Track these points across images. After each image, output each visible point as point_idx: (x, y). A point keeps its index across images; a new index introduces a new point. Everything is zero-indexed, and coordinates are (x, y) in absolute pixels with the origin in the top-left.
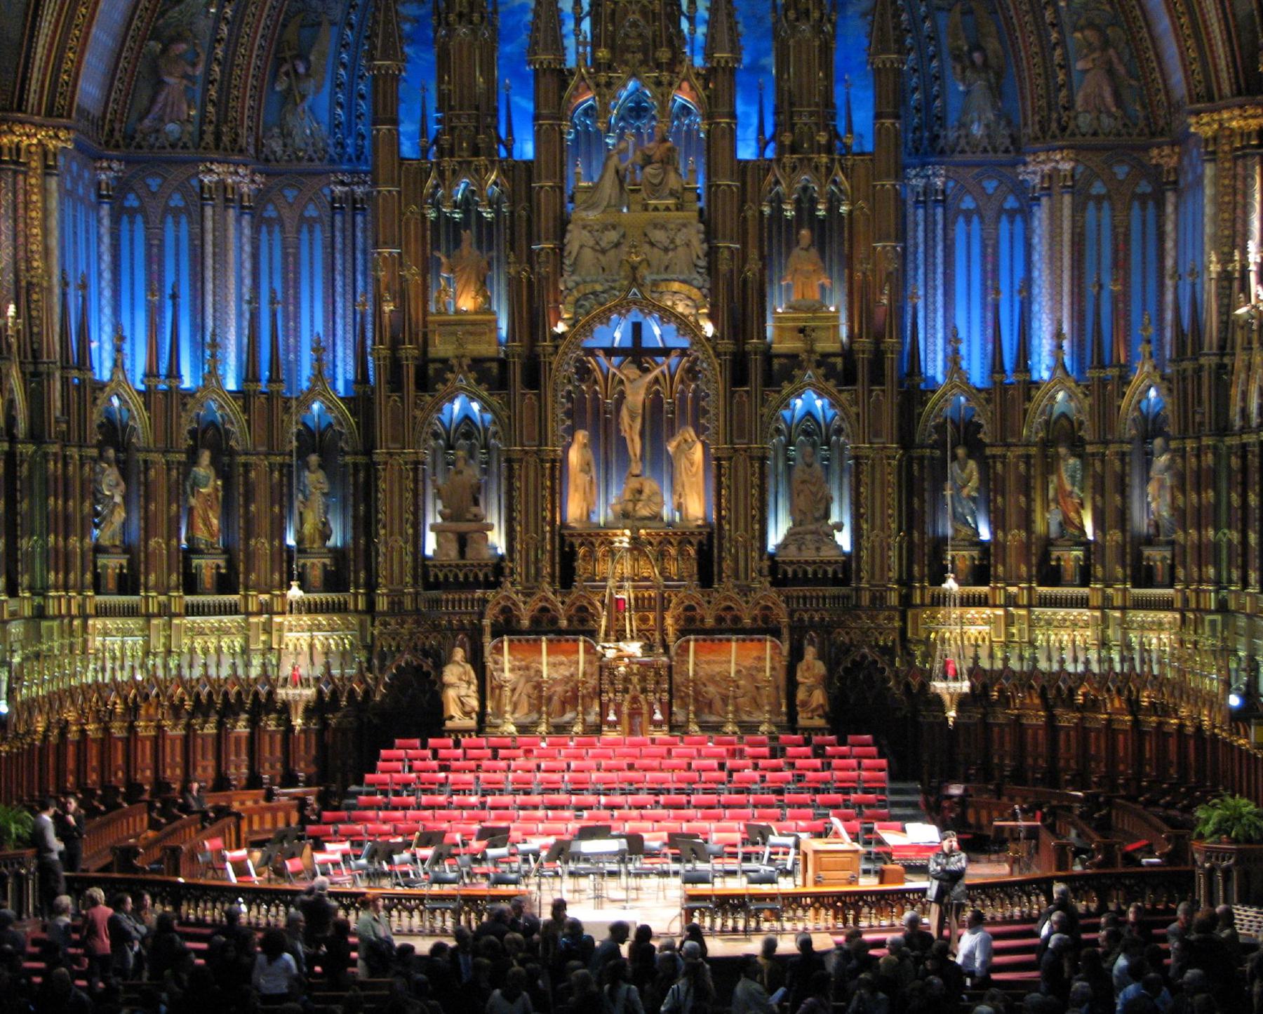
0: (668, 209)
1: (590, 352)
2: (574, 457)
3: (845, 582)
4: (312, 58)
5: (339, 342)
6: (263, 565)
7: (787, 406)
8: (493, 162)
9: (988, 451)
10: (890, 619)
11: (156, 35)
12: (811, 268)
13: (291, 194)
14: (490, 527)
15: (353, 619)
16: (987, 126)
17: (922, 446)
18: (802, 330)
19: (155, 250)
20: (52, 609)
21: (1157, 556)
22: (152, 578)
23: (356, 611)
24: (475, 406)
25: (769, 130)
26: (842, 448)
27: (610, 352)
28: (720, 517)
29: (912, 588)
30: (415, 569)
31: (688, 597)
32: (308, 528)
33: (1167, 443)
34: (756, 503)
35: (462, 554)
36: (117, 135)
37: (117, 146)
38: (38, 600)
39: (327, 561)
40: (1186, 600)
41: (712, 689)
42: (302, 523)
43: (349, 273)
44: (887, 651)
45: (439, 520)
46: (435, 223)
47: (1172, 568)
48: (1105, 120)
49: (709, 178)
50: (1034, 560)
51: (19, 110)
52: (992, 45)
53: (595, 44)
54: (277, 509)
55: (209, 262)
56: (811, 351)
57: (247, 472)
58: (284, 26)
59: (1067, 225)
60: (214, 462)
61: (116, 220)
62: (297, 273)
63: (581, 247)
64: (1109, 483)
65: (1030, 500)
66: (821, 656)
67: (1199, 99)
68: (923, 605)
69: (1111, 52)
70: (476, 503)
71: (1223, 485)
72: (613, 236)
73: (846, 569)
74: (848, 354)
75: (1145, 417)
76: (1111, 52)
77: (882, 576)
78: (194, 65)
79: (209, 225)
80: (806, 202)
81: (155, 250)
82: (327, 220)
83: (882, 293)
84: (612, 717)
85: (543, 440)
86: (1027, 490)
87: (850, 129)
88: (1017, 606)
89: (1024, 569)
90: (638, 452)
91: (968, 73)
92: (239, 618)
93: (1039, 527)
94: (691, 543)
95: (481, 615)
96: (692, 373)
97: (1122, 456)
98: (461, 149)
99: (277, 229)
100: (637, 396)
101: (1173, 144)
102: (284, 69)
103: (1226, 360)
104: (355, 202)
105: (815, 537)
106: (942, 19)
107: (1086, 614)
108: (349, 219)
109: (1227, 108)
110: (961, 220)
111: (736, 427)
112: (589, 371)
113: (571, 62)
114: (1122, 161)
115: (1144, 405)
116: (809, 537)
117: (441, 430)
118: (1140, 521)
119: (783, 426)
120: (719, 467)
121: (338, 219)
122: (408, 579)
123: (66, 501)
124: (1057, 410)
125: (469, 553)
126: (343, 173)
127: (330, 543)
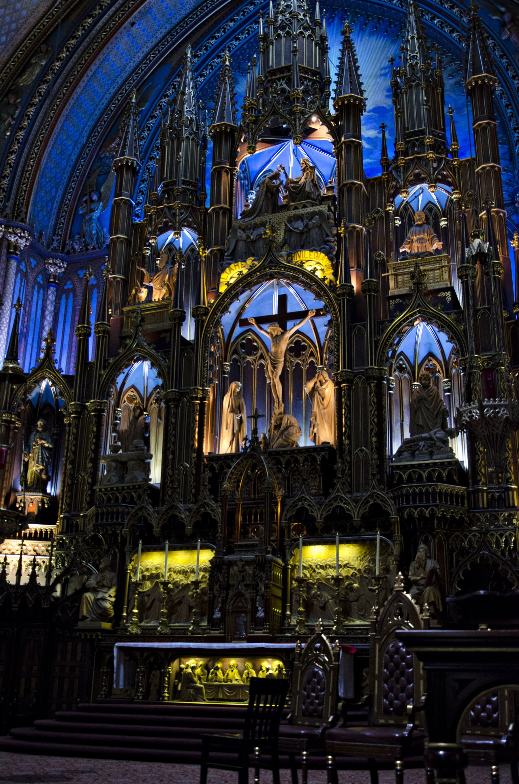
0: (305, 206)
1: (244, 322)
4: (102, 190)
12: (426, 236)
27: (261, 320)
35: (122, 479)
41: (327, 596)
58: (88, 177)
63: (237, 242)
84: (217, 615)
99: (71, 295)
105: (429, 443)
112: (256, 349)
116: (422, 443)
119: (406, 365)
125: (128, 478)
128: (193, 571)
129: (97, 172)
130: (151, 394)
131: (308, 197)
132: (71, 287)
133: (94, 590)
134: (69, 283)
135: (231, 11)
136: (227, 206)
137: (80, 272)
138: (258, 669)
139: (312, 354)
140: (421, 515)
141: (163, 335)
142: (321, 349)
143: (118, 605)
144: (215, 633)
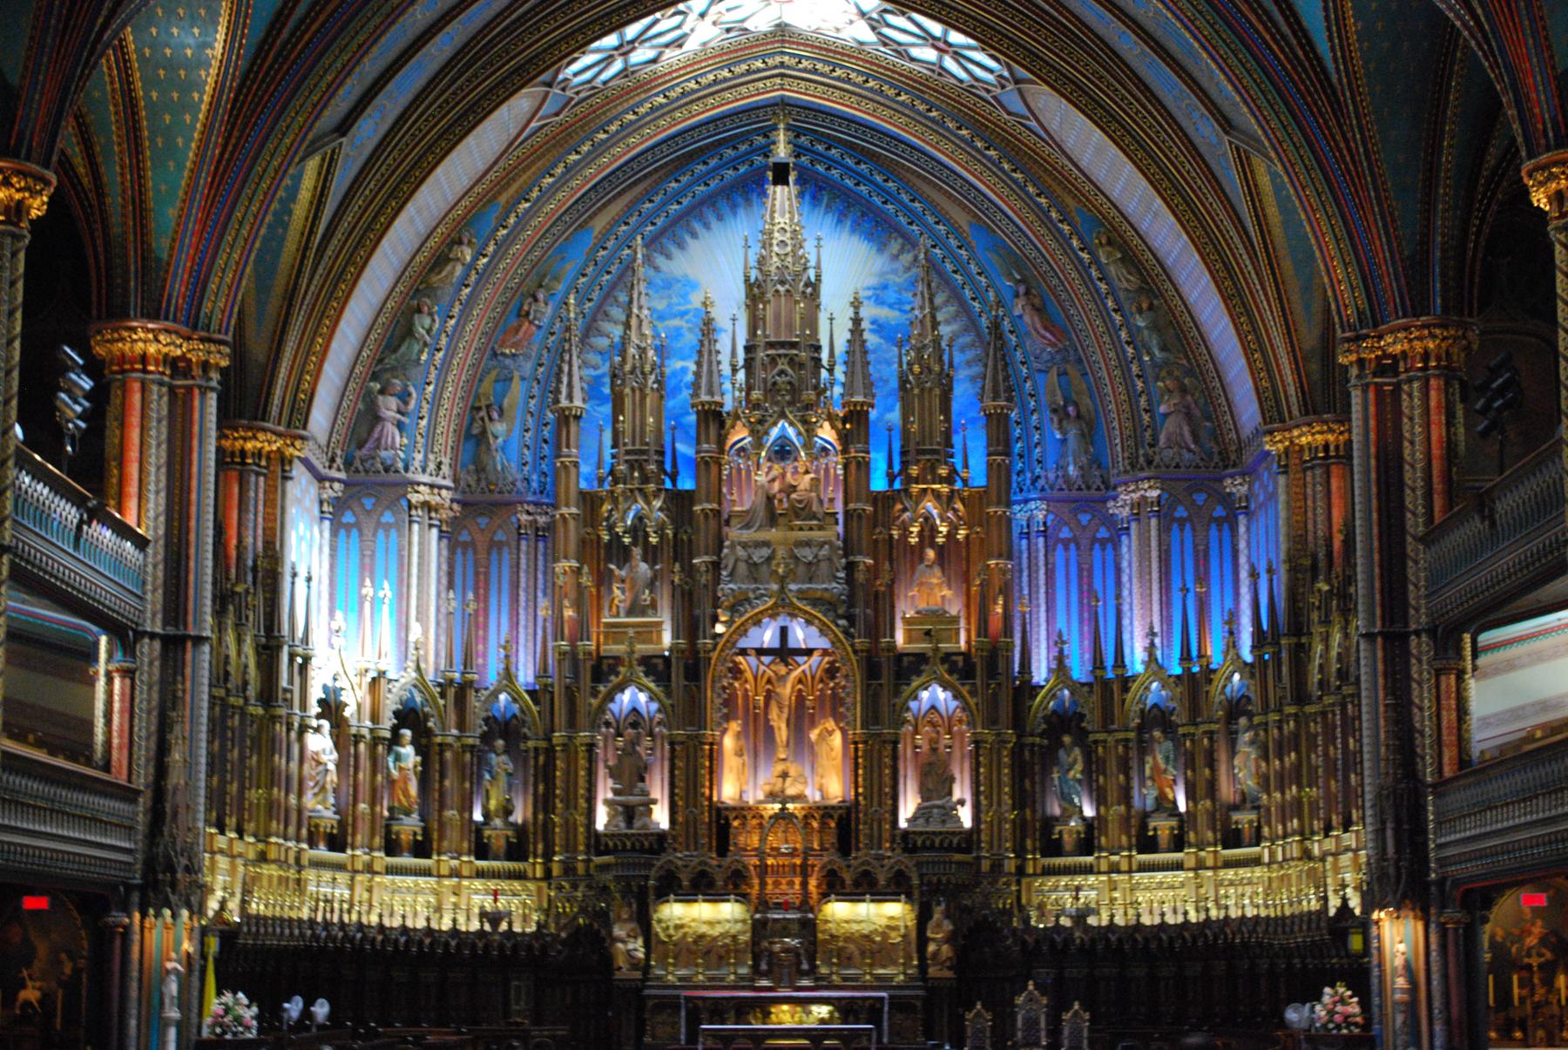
0: (811, 529)
1: (743, 652)
2: (729, 742)
3: (968, 851)
5: (521, 649)
6: (453, 834)
7: (916, 698)
8: (659, 490)
9: (1092, 737)
10: (1008, 884)
11: (375, 377)
13: (483, 521)
14: (654, 802)
15: (531, 886)
16: (1081, 468)
17: (1032, 735)
18: (928, 633)
19: (367, 560)
20: (272, 854)
21: (1244, 819)
22: (359, 838)
23: (535, 878)
24: (642, 697)
25: (897, 467)
26: (962, 734)
27: (761, 652)
28: (857, 794)
29: (1025, 859)
30: (588, 838)
31: (830, 862)
32: (493, 804)
33: (1250, 719)
34: (887, 780)
36: (339, 461)
37: (339, 470)
38: (261, 846)
39: (510, 833)
40: (1272, 854)
41: (852, 947)
42: (488, 798)
43: (531, 590)
44: (1006, 913)
45: (610, 795)
46: (609, 544)
47: (1259, 828)
48: (1187, 455)
49: (846, 503)
50: (1133, 831)
51: (263, 420)
52: (1086, 401)
53: (749, 388)
54: (467, 785)
55: (414, 570)
56: (937, 649)
57: (441, 753)
59: (1154, 543)
60: (414, 742)
61: (334, 533)
62: (487, 589)
63: (737, 561)
64: (1200, 760)
65: (1128, 778)
66: (947, 915)
67: (1272, 421)
68: (1035, 874)
69: (1189, 398)
70: (642, 779)
71: (1304, 750)
72: (765, 552)
73: (969, 840)
74: (966, 656)
75: (1230, 701)
76: (1189, 398)
77: (1000, 846)
78: (406, 403)
79: (415, 538)
80: (929, 530)
81: (367, 560)
82: (514, 544)
83: (996, 603)
84: (764, 967)
85: (702, 725)
86: (1125, 768)
87: (966, 466)
88: (1119, 872)
89: (1124, 839)
90: (784, 738)
91: (1065, 423)
92: (432, 880)
93: (1137, 802)
94: (831, 817)
95: (647, 878)
96: (831, 672)
97: (1210, 734)
98: (633, 478)
100: (786, 691)
101: (1243, 475)
102: (483, 413)
103: (1304, 640)
104: (537, 529)
106: (1038, 376)
107: (1182, 876)
108: (532, 543)
109: (1297, 426)
110: (1060, 547)
111: (872, 716)
112: (741, 672)
113: (728, 406)
114: (1200, 490)
115: (1228, 690)
117: (612, 720)
118: (1227, 792)
120: (856, 750)
121: (523, 544)
122: (581, 848)
123: (288, 762)
124: (1150, 702)
125: (637, 823)
126: (529, 503)
127: (512, 819)
128: (719, 922)
129: (494, 374)
130: (627, 716)
131: (814, 517)
132: (468, 539)
133: (623, 942)
134: (465, 532)
135: (677, 168)
136: (715, 506)
137: (480, 520)
138: (809, 1013)
139: (800, 681)
140: (939, 881)
141: (655, 661)
142: (813, 678)
143: (648, 954)
144: (765, 983)
